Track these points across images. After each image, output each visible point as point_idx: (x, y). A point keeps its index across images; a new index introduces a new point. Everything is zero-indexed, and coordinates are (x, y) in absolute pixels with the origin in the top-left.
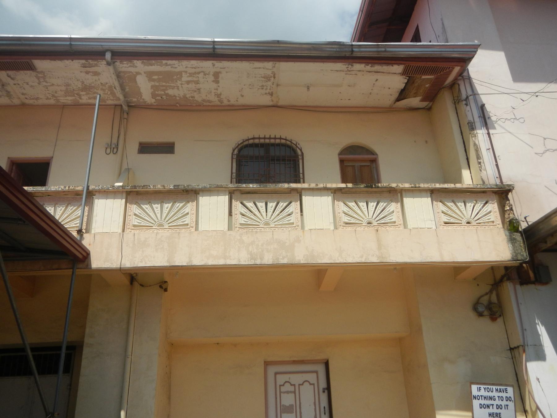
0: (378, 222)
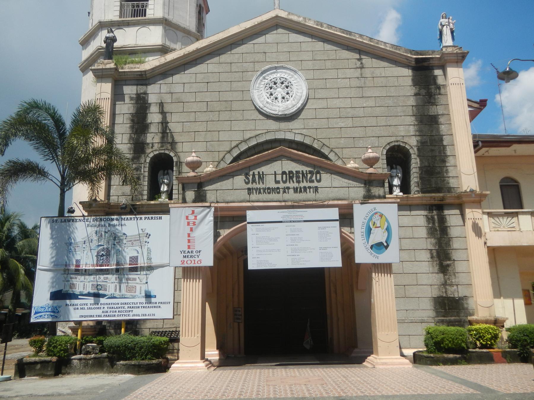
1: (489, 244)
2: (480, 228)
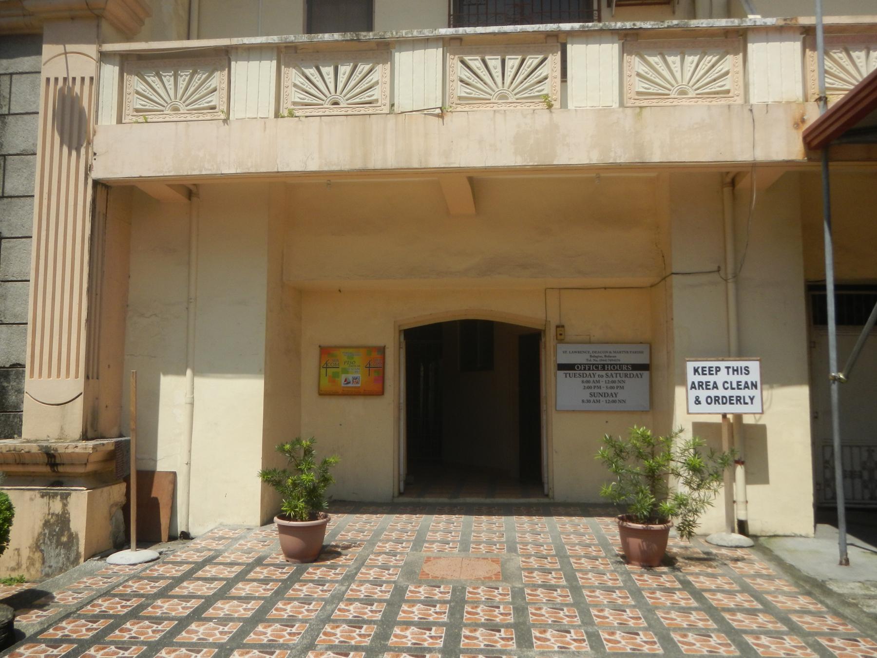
0: (699, 91)
1: (97, 174)
2: (81, 111)
